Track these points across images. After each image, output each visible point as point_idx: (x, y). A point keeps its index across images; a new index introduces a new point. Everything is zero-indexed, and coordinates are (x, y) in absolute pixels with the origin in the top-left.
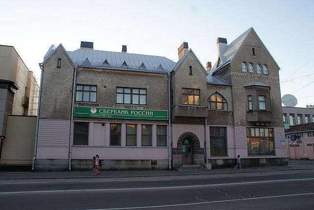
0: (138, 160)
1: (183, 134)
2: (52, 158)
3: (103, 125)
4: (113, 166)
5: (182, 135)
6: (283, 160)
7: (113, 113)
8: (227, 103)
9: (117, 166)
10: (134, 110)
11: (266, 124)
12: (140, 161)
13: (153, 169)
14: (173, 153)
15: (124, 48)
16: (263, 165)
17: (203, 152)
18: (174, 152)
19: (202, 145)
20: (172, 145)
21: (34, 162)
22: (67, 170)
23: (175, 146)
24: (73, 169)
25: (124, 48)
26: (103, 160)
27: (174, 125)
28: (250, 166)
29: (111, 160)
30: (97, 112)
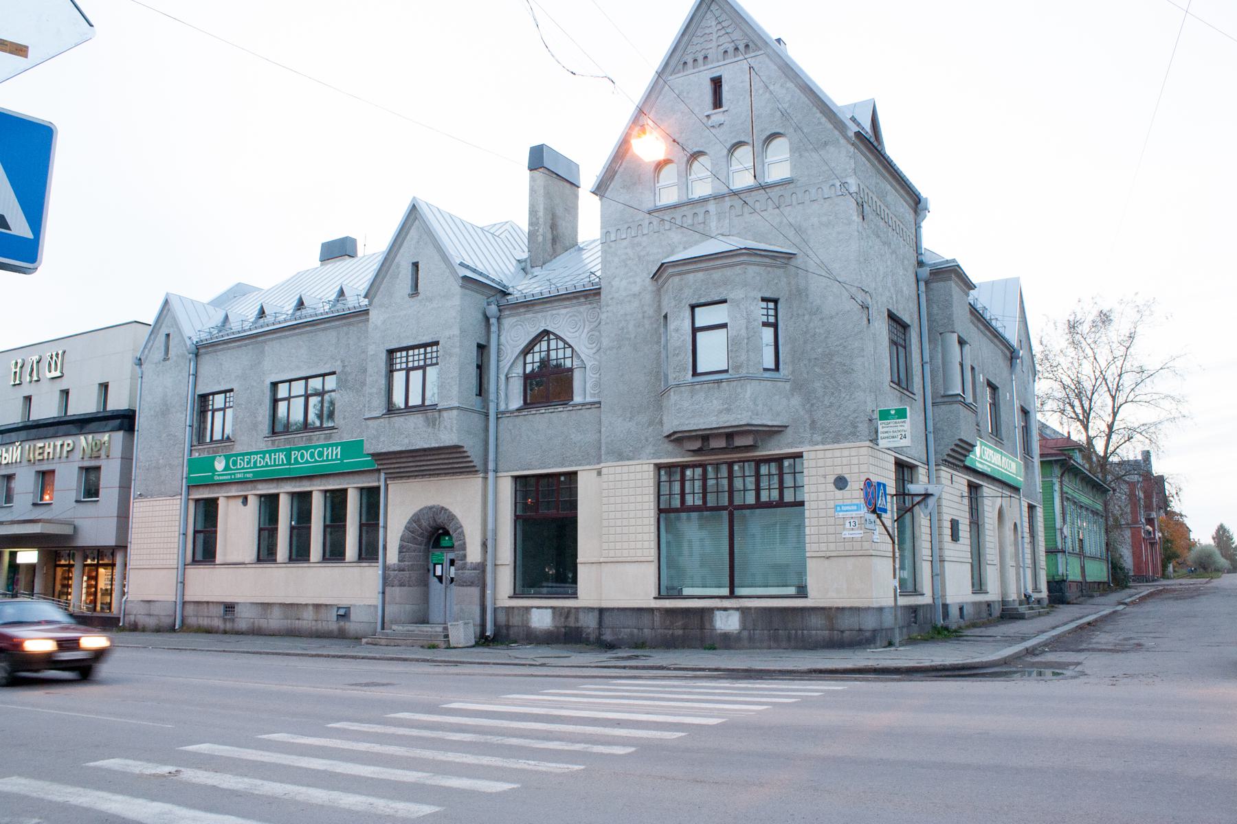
0: (306, 605)
3: (245, 500)
5: (416, 519)
6: (846, 622)
7: (255, 463)
9: (263, 623)
10: (299, 449)
11: (739, 442)
12: (311, 608)
13: (341, 635)
14: (386, 581)
16: (727, 642)
17: (480, 577)
19: (474, 554)
20: (385, 555)
22: (172, 629)
23: (393, 557)
24: (186, 628)
26: (237, 603)
28: (670, 644)
30: (227, 468)
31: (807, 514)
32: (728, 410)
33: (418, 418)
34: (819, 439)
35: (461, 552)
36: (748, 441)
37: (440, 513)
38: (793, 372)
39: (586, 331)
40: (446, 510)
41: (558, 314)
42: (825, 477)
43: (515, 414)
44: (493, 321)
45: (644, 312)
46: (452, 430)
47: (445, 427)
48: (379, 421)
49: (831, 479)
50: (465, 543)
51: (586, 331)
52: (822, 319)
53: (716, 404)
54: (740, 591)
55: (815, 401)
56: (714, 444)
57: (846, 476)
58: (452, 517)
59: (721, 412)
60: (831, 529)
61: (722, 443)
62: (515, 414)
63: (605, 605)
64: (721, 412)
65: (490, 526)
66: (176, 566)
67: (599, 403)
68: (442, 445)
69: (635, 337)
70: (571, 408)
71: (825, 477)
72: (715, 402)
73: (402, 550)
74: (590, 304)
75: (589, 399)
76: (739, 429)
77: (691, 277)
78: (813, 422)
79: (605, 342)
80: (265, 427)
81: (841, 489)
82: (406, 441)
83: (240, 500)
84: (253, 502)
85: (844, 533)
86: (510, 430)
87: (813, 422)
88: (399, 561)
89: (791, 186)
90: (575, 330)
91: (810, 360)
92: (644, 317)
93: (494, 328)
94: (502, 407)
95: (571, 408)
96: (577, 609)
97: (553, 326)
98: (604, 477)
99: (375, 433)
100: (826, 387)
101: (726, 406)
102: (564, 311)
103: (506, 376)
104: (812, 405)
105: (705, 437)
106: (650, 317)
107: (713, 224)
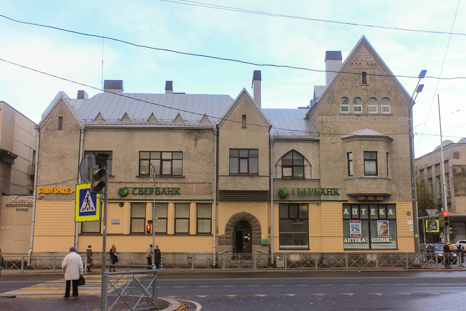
1: (230, 219)
2: (52, 251)
3: (122, 205)
4: (134, 261)
5: (234, 217)
8: (311, 166)
11: (378, 199)
15: (169, 86)
18: (220, 241)
20: (217, 232)
21: (29, 255)
23: (222, 232)
25: (169, 86)
27: (220, 204)
29: (131, 253)
31: (398, 223)
32: (378, 188)
33: (249, 178)
34: (401, 199)
35: (260, 231)
36: (382, 199)
37: (248, 215)
38: (392, 177)
39: (311, 153)
40: (251, 215)
41: (299, 145)
42: (403, 211)
43: (281, 180)
44: (272, 143)
45: (338, 150)
46: (266, 184)
47: (263, 183)
48: (226, 177)
49: (406, 212)
50: (260, 228)
51: (311, 153)
52: (402, 162)
53: (375, 186)
54: (372, 248)
55: (400, 187)
56: (370, 199)
57: (410, 212)
58: (253, 217)
59: (376, 188)
60: (406, 228)
61: (372, 199)
62: (281, 180)
63: (323, 252)
64: (376, 188)
65: (272, 222)
66: (74, 235)
67: (319, 180)
68: (261, 190)
69: (334, 158)
70: (306, 180)
71: (403, 211)
72: (374, 185)
73: (227, 230)
74: (313, 143)
75: (313, 178)
76: (378, 195)
77: (364, 142)
78: (400, 194)
79: (322, 158)
80: (136, 172)
81: (409, 216)
82: (243, 187)
83: (118, 205)
84: (127, 205)
85: (410, 229)
86: (278, 186)
87: (400, 194)
88: (226, 234)
89: (392, 116)
90: (305, 151)
91: (398, 174)
92: (338, 152)
93: (272, 146)
94: (274, 177)
95: (306, 180)
96: (310, 253)
97: (297, 149)
98: (322, 207)
99: (225, 182)
100: (403, 183)
101: (378, 187)
102: (302, 144)
103: (275, 165)
104: (399, 189)
105: (366, 196)
106: (340, 152)
107: (364, 124)
